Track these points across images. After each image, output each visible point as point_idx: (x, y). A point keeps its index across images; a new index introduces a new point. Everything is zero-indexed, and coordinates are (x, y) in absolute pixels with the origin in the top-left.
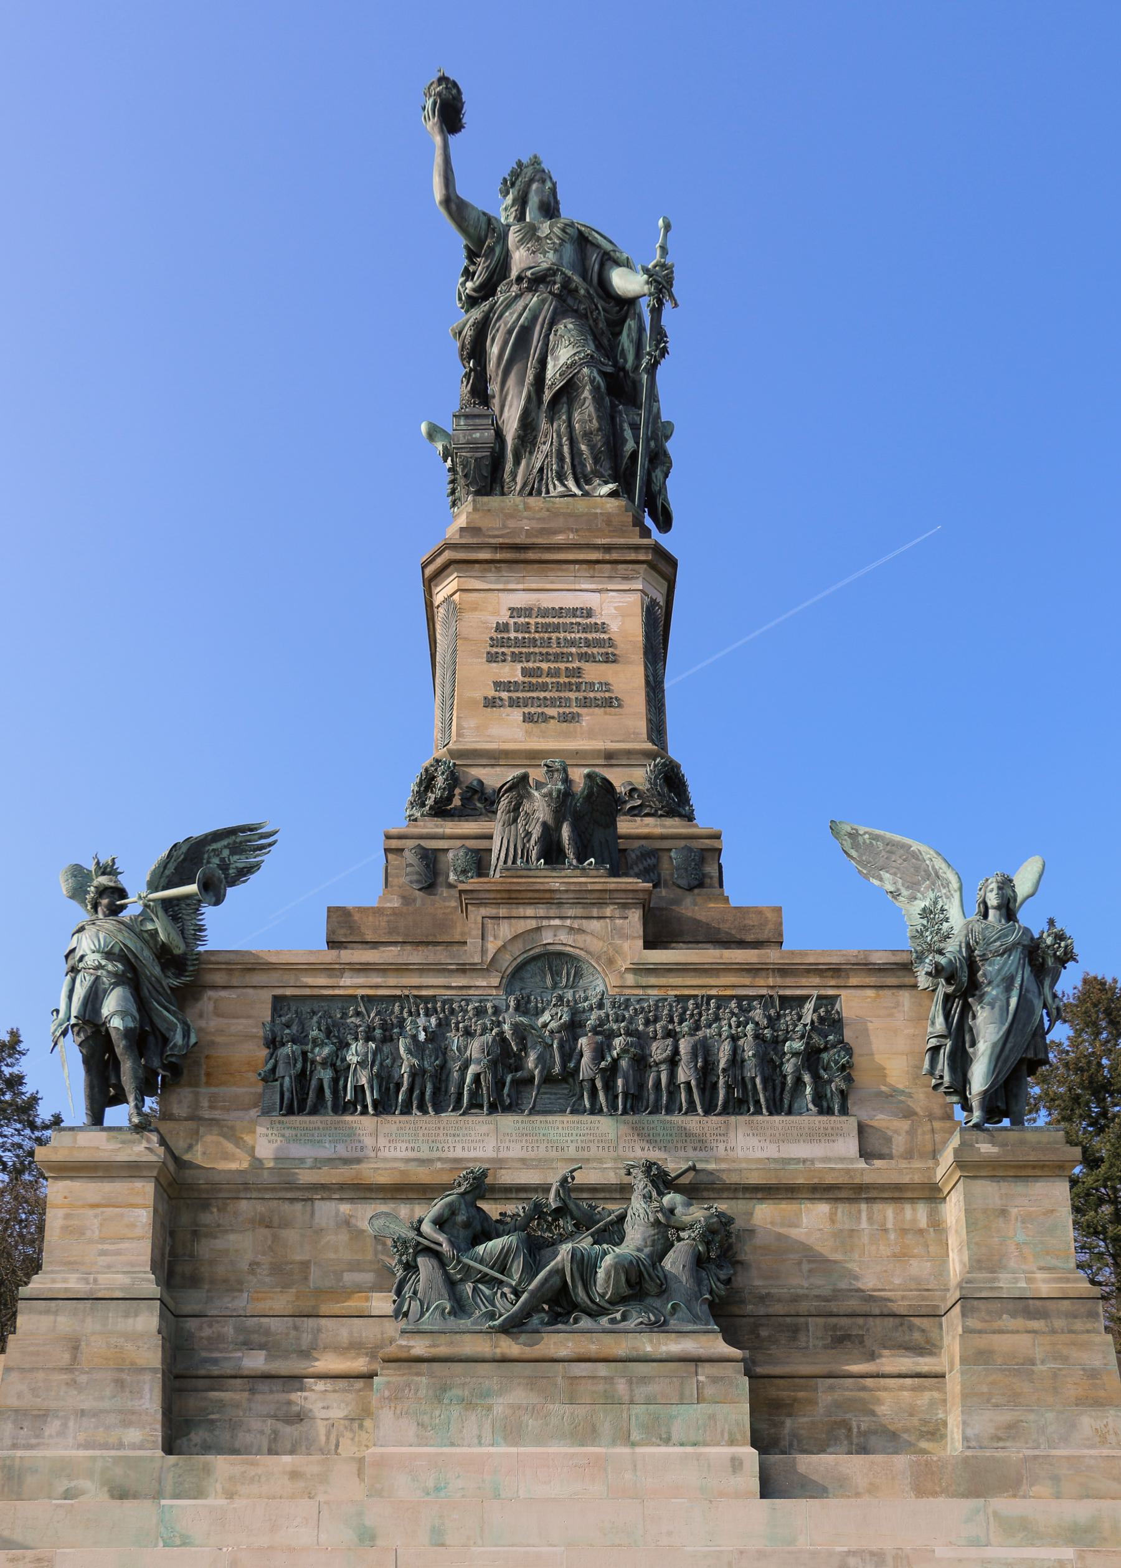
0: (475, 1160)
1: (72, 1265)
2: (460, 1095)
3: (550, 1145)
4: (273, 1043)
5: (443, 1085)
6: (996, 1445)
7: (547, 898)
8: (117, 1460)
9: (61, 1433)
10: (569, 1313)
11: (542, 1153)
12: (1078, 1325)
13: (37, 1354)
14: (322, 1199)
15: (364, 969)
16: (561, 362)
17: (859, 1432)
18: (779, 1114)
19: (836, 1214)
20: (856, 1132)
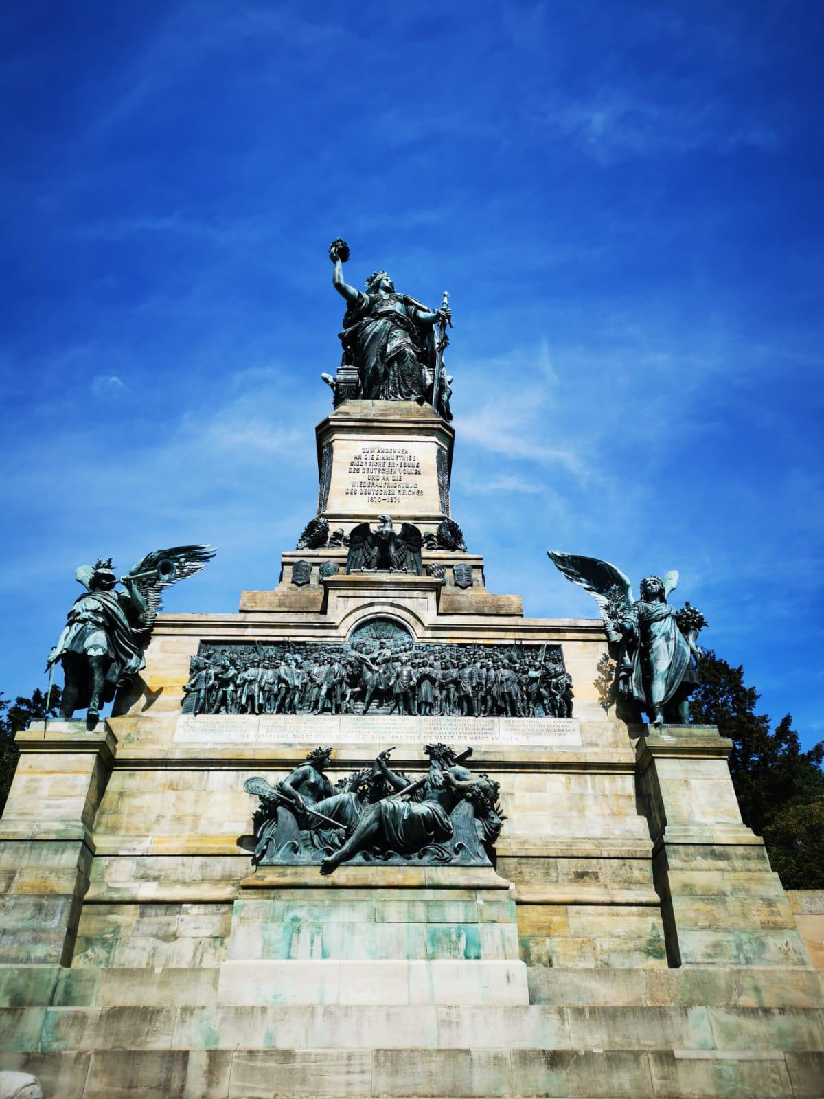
2: (317, 702)
4: (195, 669)
6: (707, 960)
8: (22, 972)
11: (368, 740)
17: (602, 950)
20: (578, 729)
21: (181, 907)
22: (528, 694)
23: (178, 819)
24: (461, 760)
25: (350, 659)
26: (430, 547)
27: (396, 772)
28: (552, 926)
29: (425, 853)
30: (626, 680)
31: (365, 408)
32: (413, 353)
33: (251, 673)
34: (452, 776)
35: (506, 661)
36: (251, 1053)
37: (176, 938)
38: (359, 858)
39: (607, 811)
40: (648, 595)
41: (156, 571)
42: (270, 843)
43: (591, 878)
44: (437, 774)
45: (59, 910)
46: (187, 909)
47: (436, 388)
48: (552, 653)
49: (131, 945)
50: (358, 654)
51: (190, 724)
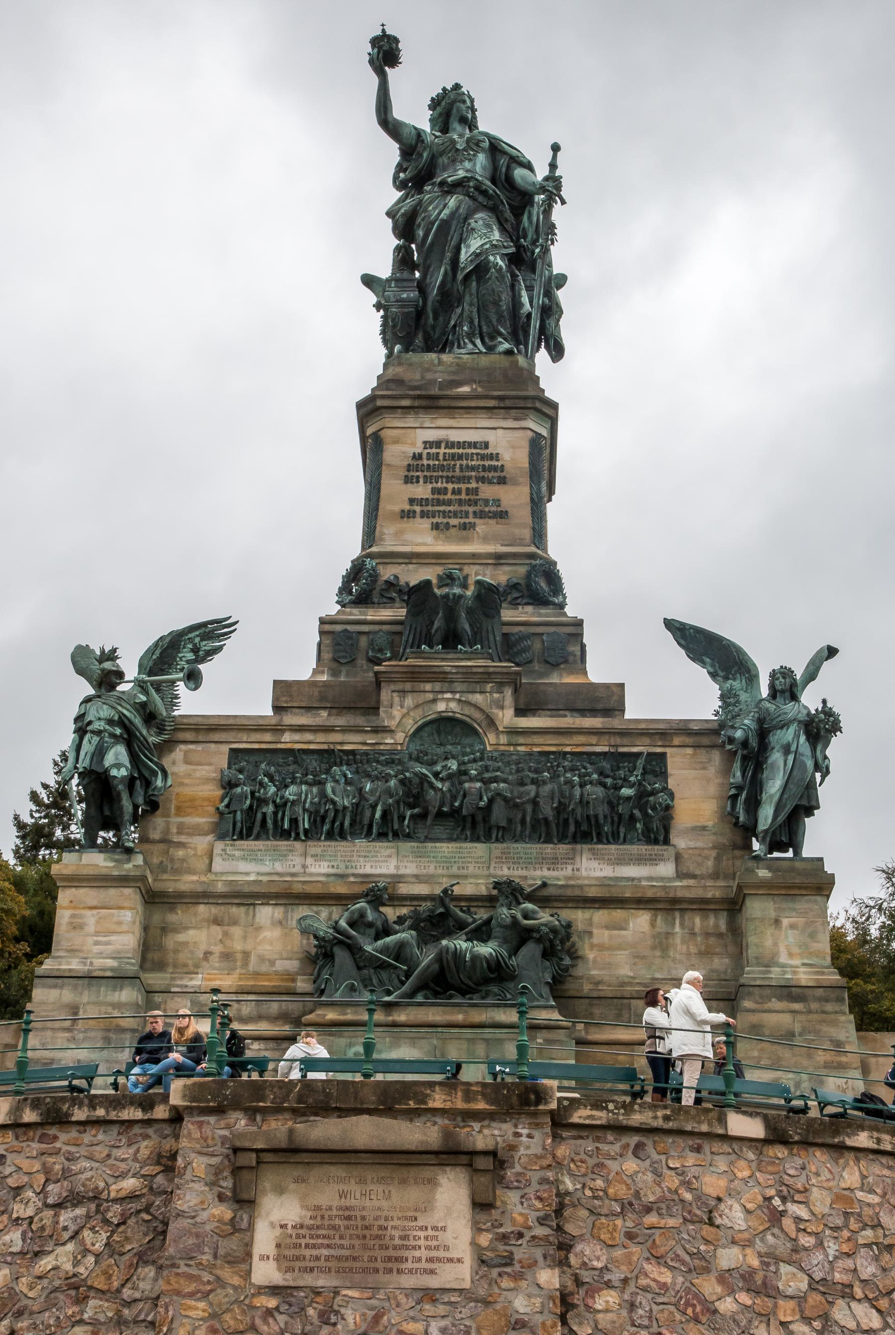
0: (380, 876)
1: (72, 951)
2: (370, 826)
4: (229, 785)
7: (441, 677)
10: (445, 992)
11: (431, 870)
12: (829, 1007)
15: (300, 729)
16: (472, 250)
20: (673, 859)
23: (227, 956)
24: (531, 897)
26: (514, 604)
30: (734, 798)
31: (428, 370)
33: (291, 793)
34: (519, 916)
35: (595, 776)
38: (419, 998)
39: (693, 949)
40: (774, 693)
44: (504, 913)
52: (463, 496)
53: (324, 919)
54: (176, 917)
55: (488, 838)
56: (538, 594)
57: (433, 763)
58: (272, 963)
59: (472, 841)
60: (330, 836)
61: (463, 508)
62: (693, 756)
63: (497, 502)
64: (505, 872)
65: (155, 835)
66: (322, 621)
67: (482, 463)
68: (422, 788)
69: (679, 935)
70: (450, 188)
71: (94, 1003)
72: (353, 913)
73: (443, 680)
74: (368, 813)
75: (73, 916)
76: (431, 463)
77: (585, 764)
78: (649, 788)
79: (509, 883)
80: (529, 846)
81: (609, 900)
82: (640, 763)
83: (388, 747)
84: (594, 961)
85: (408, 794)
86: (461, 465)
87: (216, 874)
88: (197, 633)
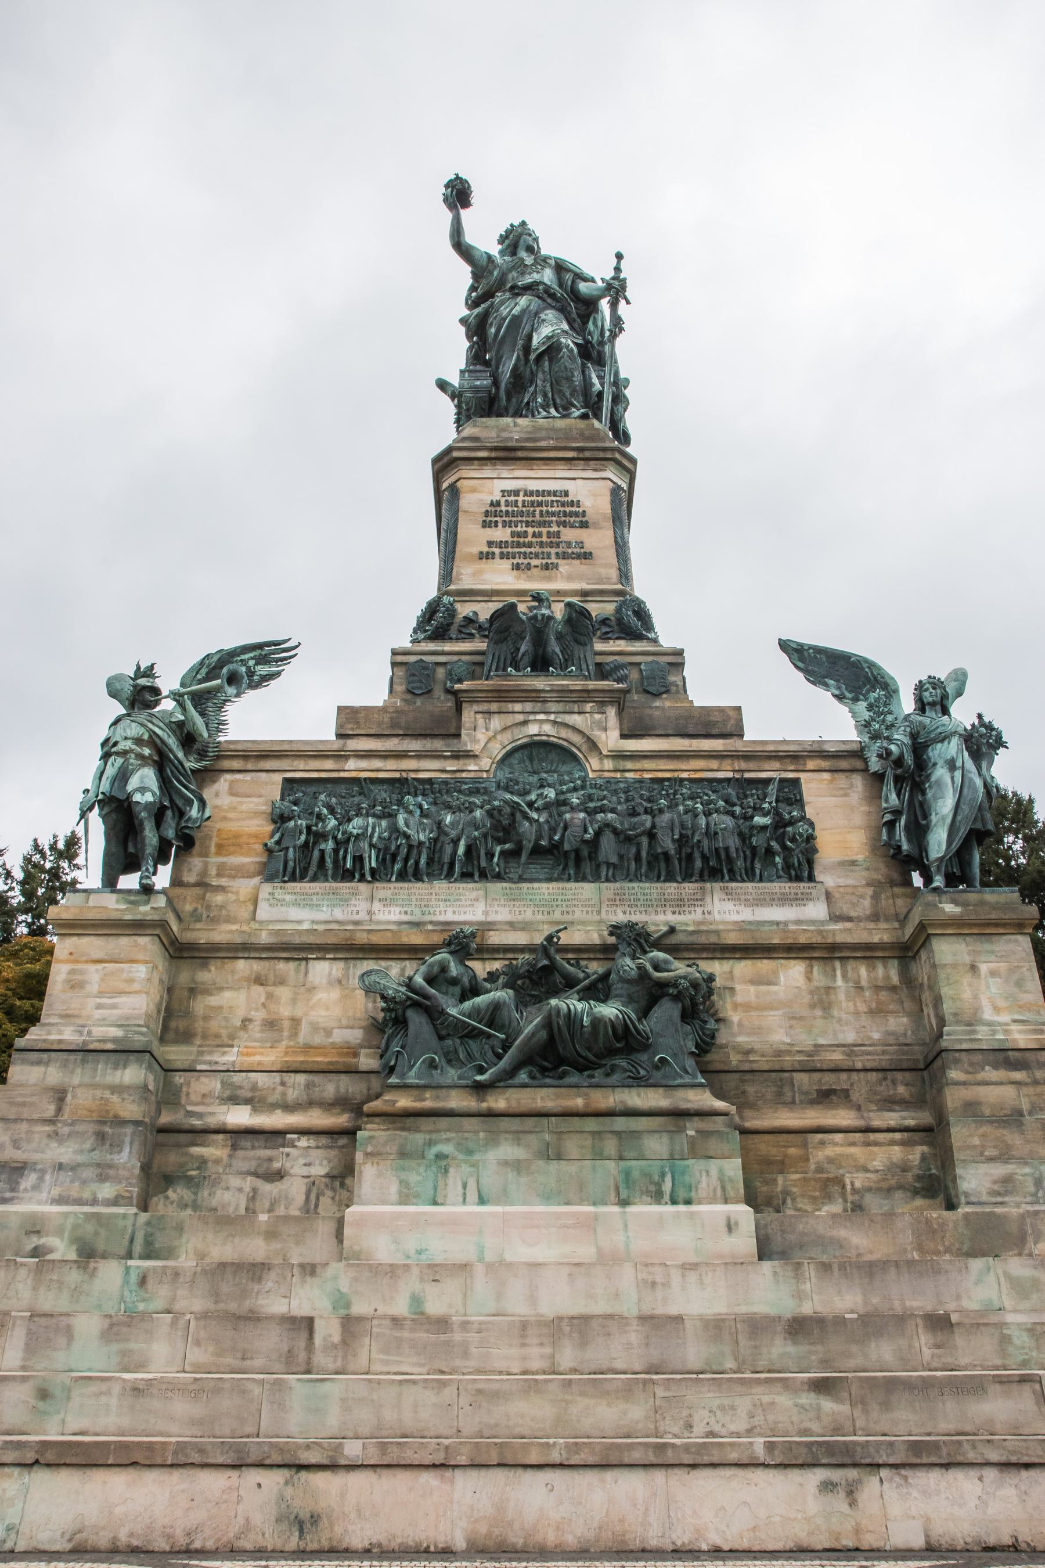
0: (465, 923)
2: (452, 865)
3: (536, 909)
4: (280, 819)
5: (436, 856)
6: (994, 1200)
7: (533, 696)
8: (89, 1216)
9: (36, 1187)
10: (556, 1068)
11: (528, 915)
13: (24, 1104)
14: (317, 959)
16: (543, 335)
17: (853, 1189)
18: (752, 881)
19: (811, 972)
20: (823, 897)
21: (285, 1138)
22: (754, 849)
23: (271, 1024)
24: (657, 945)
25: (496, 803)
26: (605, 638)
27: (568, 961)
28: (787, 1161)
29: (613, 1069)
30: (891, 825)
31: (504, 430)
32: (572, 345)
33: (355, 826)
35: (721, 803)
36: (396, 1321)
37: (282, 1177)
38: (523, 1076)
39: (862, 1007)
40: (922, 706)
41: (219, 681)
42: (400, 1058)
43: (839, 1097)
44: (627, 964)
45: (128, 1140)
46: (293, 1140)
47: (607, 399)
48: (786, 790)
49: (223, 1184)
50: (508, 796)
51: (277, 896)
52: (544, 539)
53: (395, 973)
54: (206, 976)
55: (596, 878)
56: (631, 628)
57: (527, 793)
58: (328, 1033)
59: (577, 881)
60: (402, 877)
61: (545, 550)
62: (831, 781)
63: (581, 544)
64: (620, 917)
65: (190, 878)
66: (394, 653)
67: (562, 509)
68: (514, 821)
69: (843, 989)
70: (517, 291)
71: (90, 1088)
72: (431, 965)
73: (534, 701)
74: (448, 849)
75: (72, 972)
76: (510, 509)
77: (706, 791)
78: (787, 817)
79: (631, 926)
80: (647, 885)
81: (751, 950)
82: (772, 790)
83: (472, 775)
84: (740, 1024)
85: (497, 826)
86: (541, 511)
87: (261, 922)
88: (252, 655)
